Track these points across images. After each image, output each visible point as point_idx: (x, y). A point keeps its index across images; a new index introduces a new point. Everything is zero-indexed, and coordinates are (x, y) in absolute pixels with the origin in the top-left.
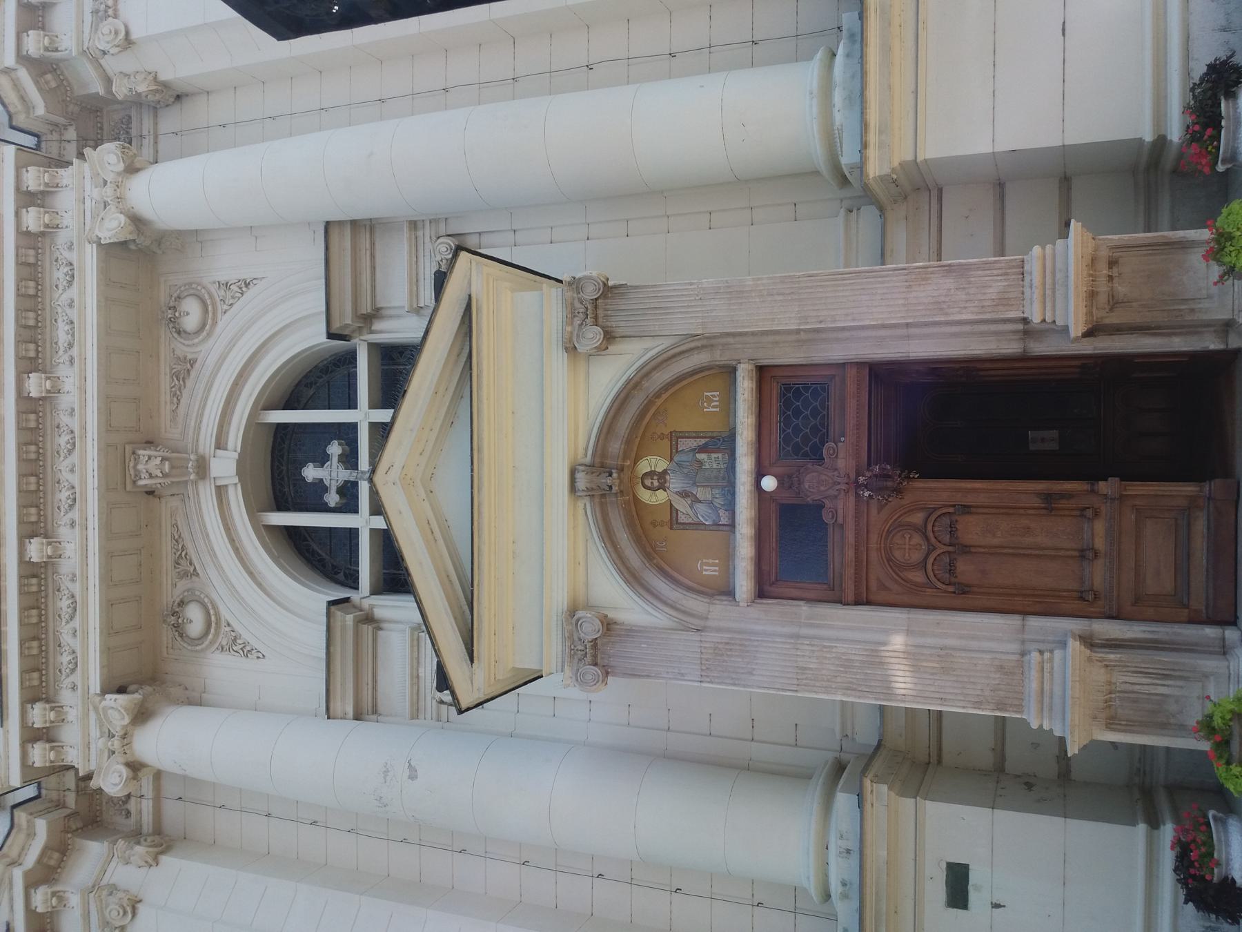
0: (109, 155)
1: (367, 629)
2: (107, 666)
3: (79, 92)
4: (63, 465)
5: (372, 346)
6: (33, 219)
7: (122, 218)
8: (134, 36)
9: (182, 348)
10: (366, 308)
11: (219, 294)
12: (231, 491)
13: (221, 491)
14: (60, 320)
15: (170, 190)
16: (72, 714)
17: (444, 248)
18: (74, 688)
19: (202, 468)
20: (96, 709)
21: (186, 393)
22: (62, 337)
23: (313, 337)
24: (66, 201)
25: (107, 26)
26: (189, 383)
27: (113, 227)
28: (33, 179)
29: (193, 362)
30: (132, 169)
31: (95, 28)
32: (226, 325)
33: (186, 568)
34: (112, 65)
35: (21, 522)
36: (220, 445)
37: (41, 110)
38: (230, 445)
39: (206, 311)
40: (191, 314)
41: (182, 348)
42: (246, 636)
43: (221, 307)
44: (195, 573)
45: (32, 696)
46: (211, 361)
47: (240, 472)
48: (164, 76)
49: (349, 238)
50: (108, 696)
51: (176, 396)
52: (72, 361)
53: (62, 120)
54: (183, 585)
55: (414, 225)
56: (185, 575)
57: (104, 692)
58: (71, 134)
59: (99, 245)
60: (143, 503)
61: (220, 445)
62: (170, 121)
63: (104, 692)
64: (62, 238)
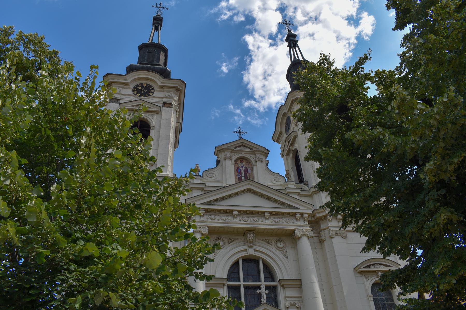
0: (311, 234)
1: (222, 286)
2: (212, 227)
3: (321, 222)
4: (252, 219)
5: (277, 285)
6: (298, 215)
7: (299, 236)
8: (333, 239)
9: (273, 241)
10: (285, 286)
11: (284, 251)
12: (246, 252)
13: (246, 250)
14: (279, 219)
15: (305, 245)
16: (202, 219)
17: (298, 304)
18: (207, 219)
19: (251, 247)
20: (205, 225)
21: (264, 243)
22: (276, 220)
23: (279, 276)
24: (301, 223)
25: (334, 234)
26: (267, 244)
27: (298, 233)
28: (306, 216)
29: (271, 245)
30: (308, 237)
31: (333, 231)
32: (278, 253)
33: (230, 241)
34: (326, 232)
35: (241, 210)
36: (255, 250)
37: (318, 215)
38: (256, 253)
39: (281, 248)
40: (281, 245)
41: (273, 241)
42: (217, 255)
43: (282, 251)
44: (229, 244)
45: (206, 210)
46: (272, 250)
47: (250, 255)
48: (325, 242)
49: (298, 284)
50: (207, 229)
51: (264, 240)
52: (272, 222)
53: (316, 218)
54: (226, 240)
55: (301, 297)
56: (228, 241)
57: (208, 227)
58: (313, 219)
59: (294, 230)
60: (243, 234)
61: (255, 250)
62: (316, 239)
63: (208, 227)
64: (294, 221)
